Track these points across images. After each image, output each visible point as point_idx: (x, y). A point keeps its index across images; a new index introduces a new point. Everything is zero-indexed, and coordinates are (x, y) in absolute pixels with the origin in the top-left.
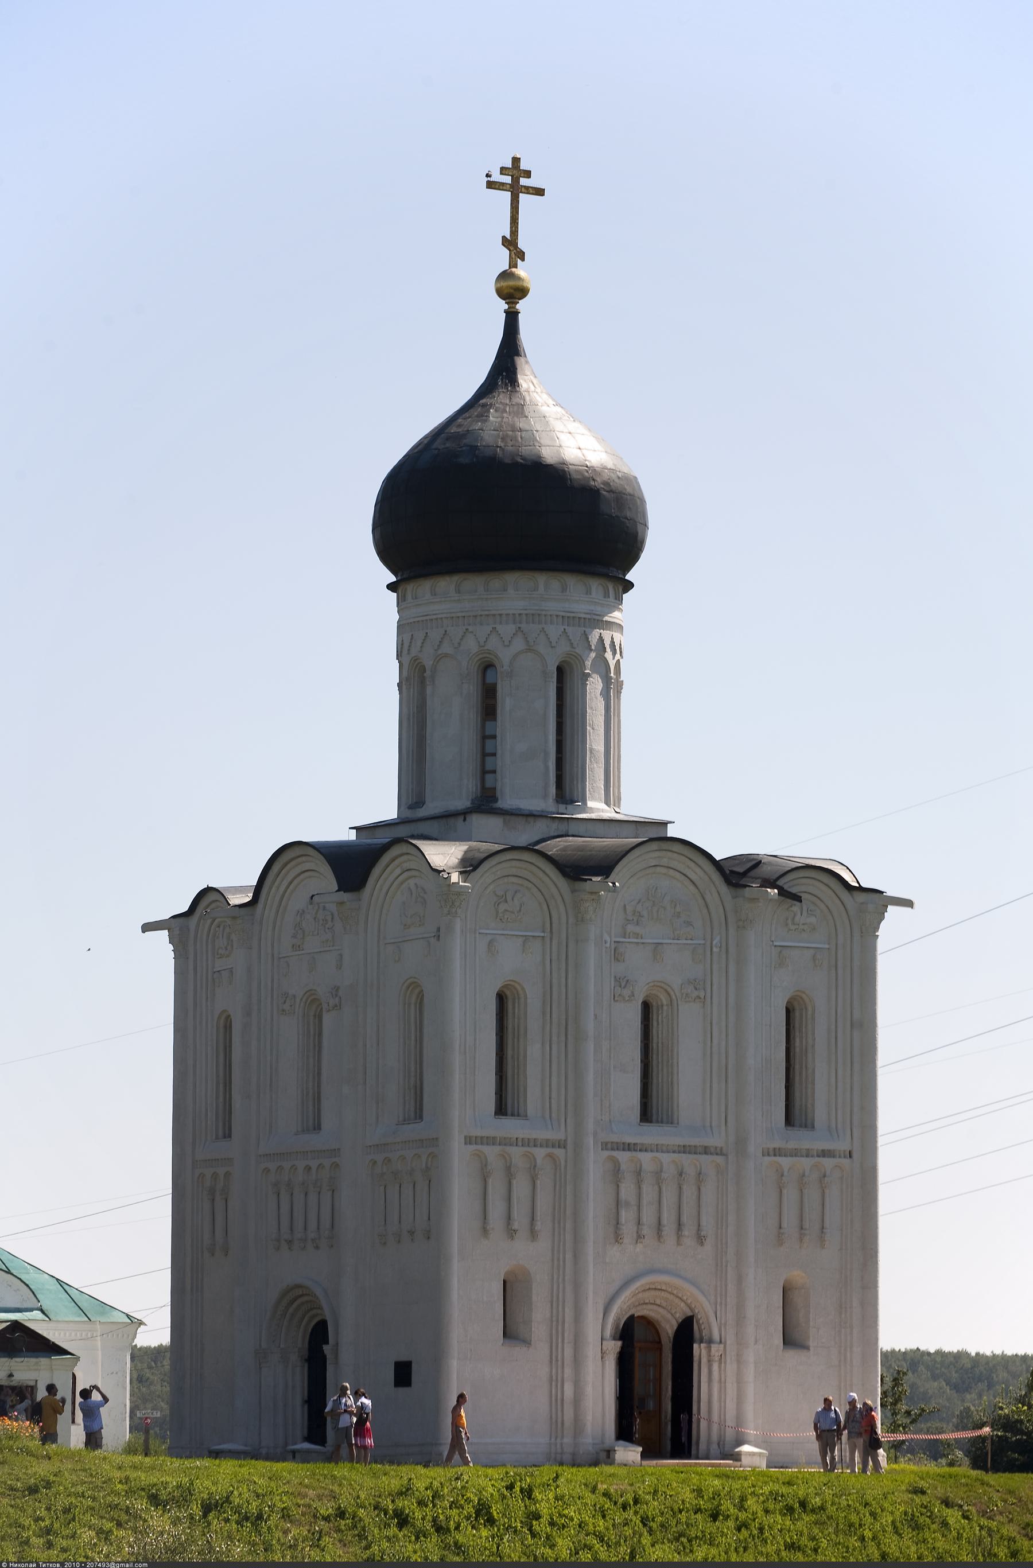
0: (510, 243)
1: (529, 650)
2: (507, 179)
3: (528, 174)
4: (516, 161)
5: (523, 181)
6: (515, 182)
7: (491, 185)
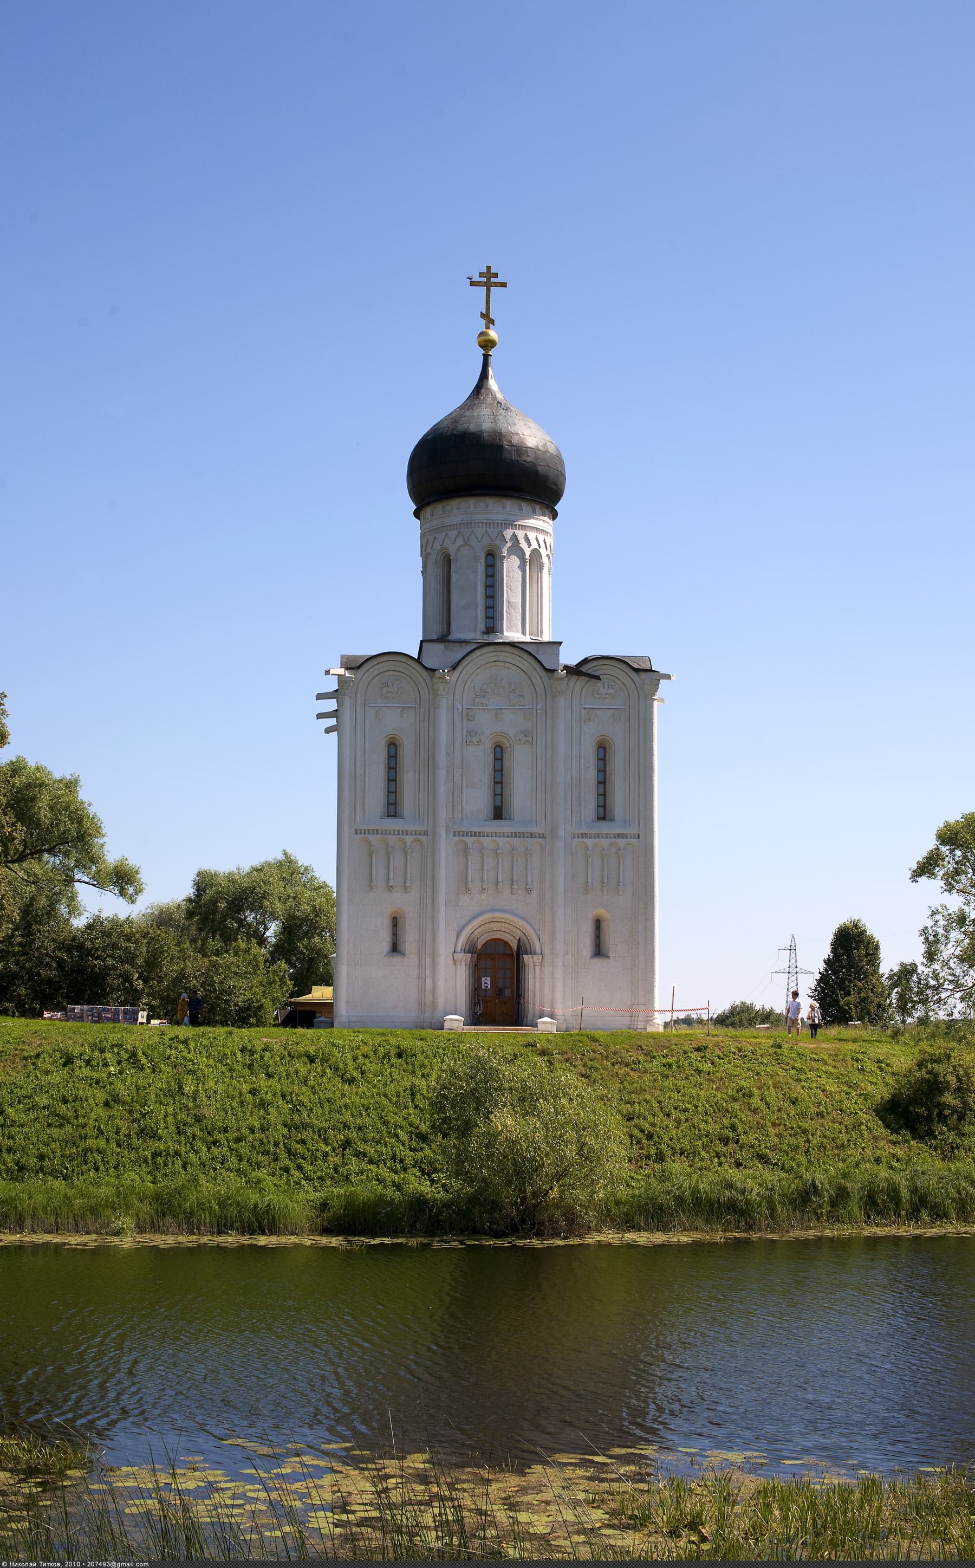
0: (486, 316)
1: (466, 544)
2: (484, 280)
3: (496, 275)
4: (489, 268)
5: (493, 280)
6: (488, 280)
7: (473, 284)
